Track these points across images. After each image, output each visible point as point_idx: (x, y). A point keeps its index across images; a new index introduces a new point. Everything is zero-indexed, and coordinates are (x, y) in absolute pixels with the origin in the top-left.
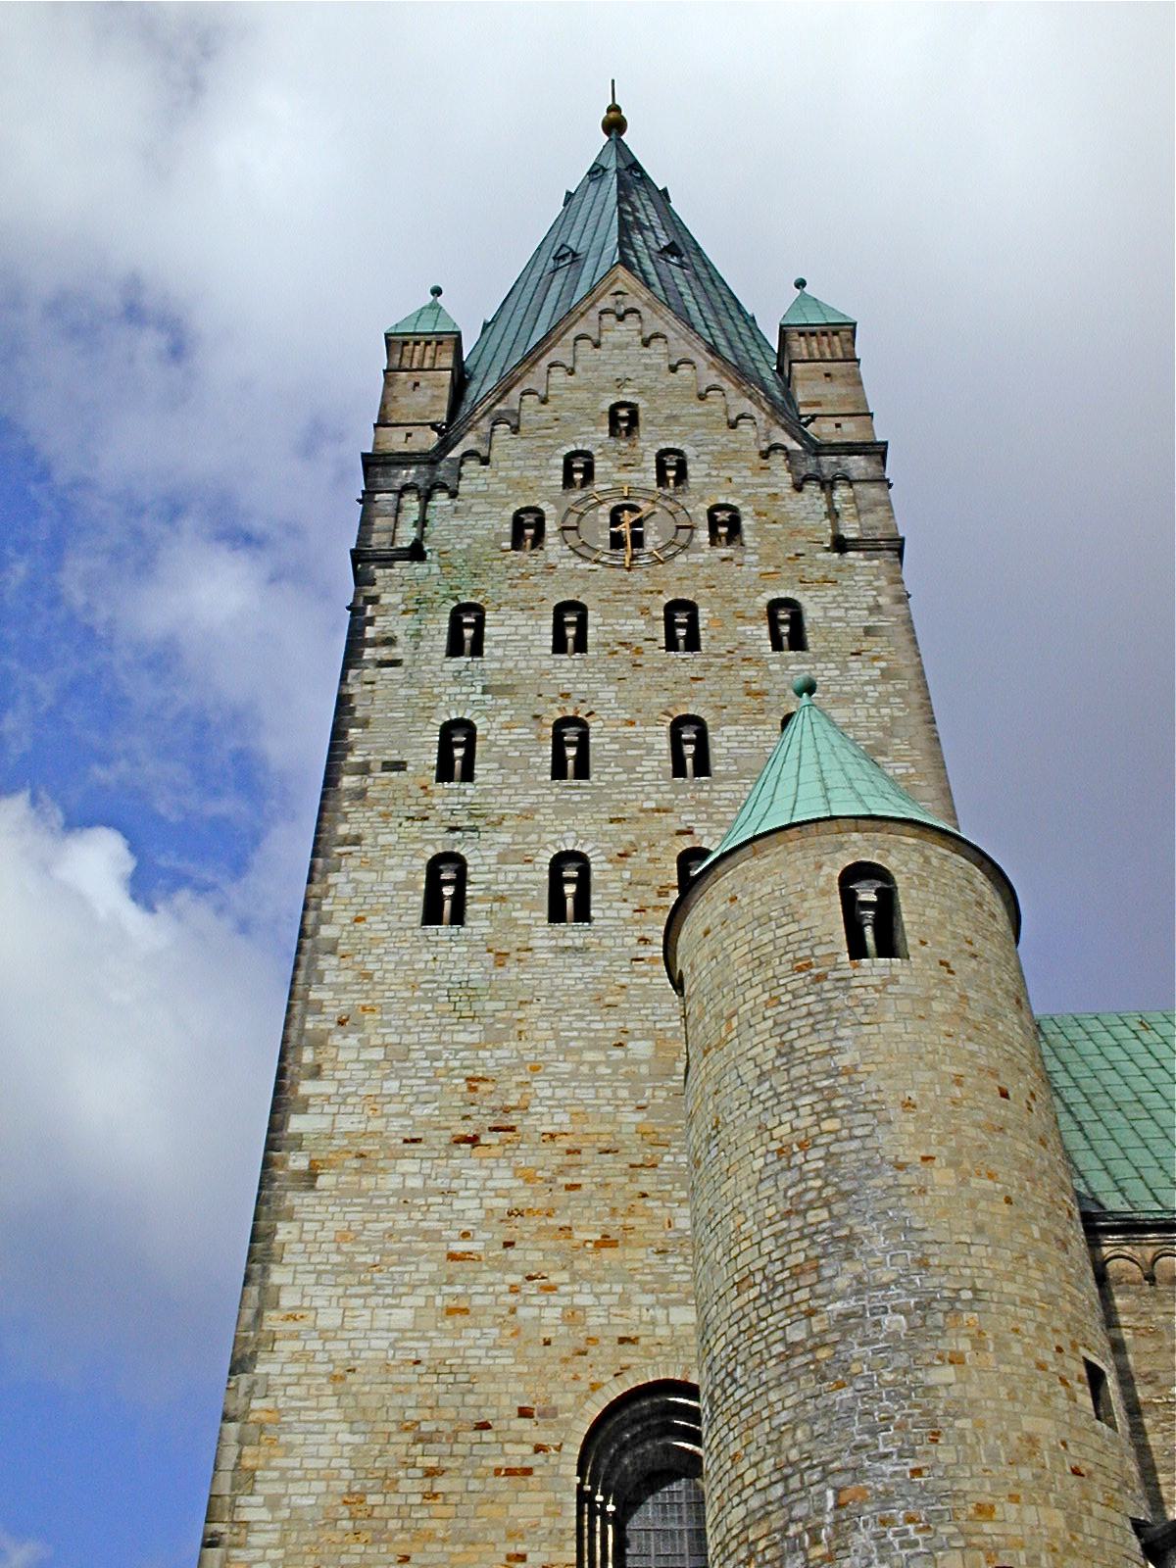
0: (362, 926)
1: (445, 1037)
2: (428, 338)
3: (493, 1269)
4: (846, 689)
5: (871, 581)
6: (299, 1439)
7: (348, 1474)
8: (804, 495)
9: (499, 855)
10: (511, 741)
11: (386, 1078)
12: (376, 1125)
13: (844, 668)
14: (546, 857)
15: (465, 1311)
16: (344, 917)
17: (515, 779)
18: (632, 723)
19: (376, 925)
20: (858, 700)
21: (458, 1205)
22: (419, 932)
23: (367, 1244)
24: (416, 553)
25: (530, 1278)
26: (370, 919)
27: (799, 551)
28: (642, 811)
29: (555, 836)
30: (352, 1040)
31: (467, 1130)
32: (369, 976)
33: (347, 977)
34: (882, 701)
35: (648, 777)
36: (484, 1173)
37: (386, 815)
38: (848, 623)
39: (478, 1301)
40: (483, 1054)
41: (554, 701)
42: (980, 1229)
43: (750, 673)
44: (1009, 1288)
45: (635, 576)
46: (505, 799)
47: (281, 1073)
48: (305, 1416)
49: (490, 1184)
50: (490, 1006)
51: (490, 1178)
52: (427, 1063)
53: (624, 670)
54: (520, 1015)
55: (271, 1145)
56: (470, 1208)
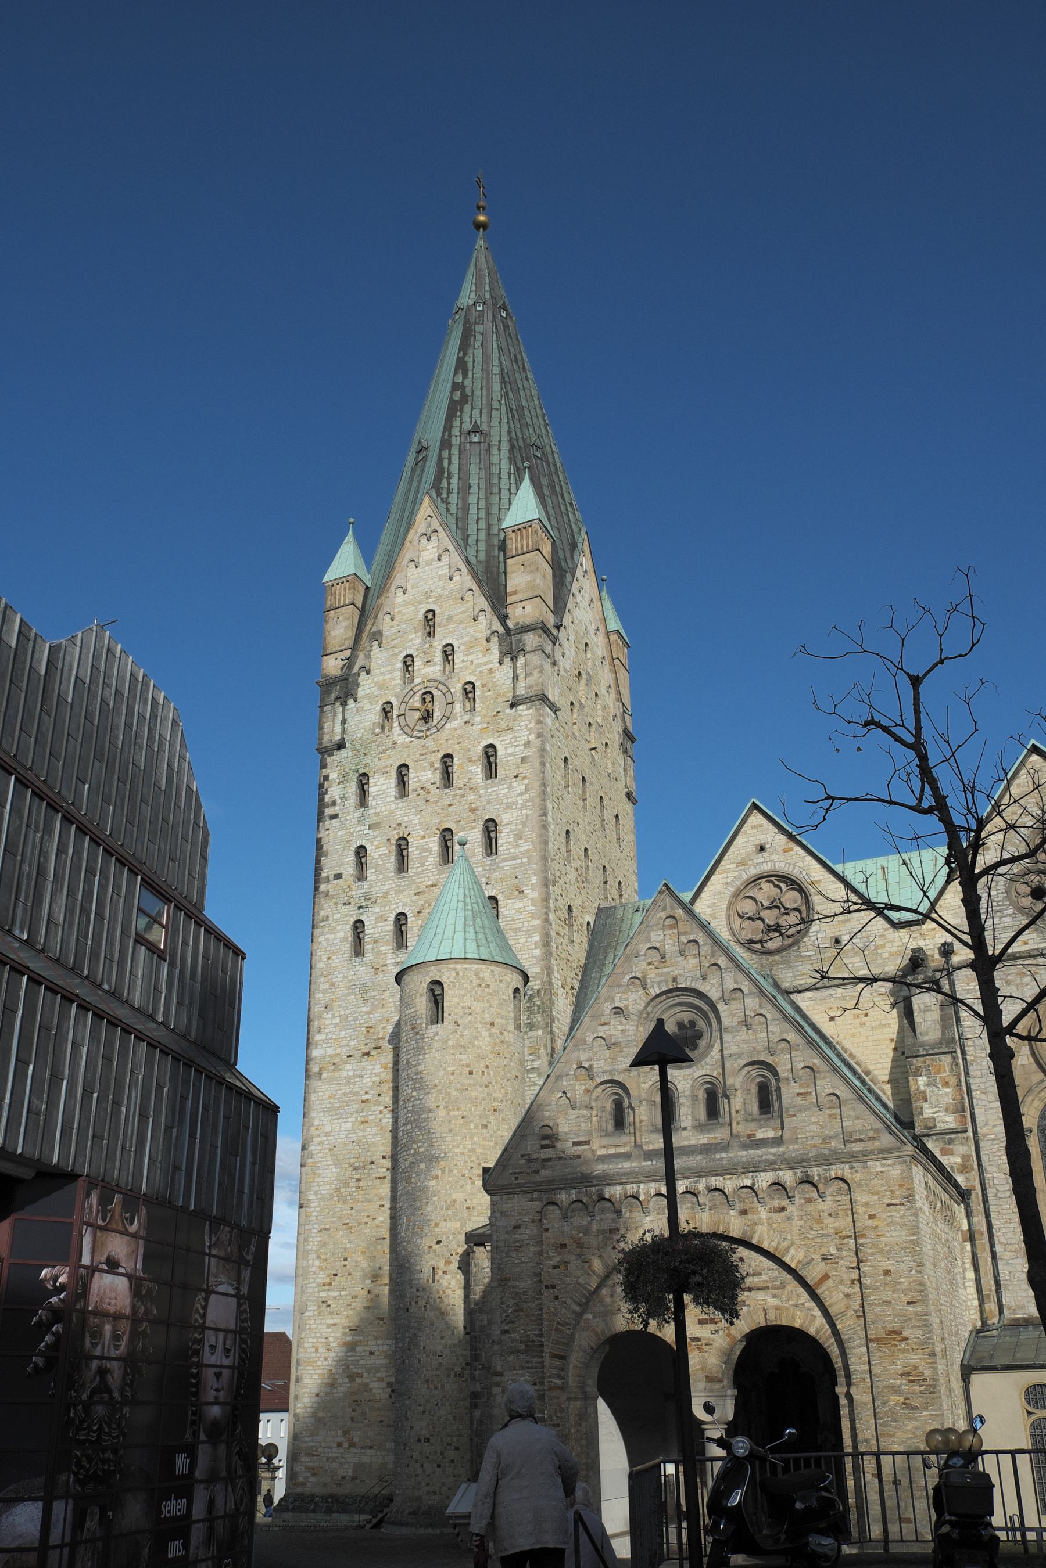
0: (331, 961)
1: (359, 1010)
2: (342, 580)
3: (375, 1105)
4: (510, 800)
5: (527, 725)
6: (321, 1172)
7: (335, 1182)
8: (503, 666)
9: (376, 919)
10: (380, 855)
11: (341, 1030)
12: (339, 1051)
13: (510, 787)
14: (392, 917)
15: (366, 1122)
16: (324, 958)
17: (381, 877)
18: (424, 837)
19: (335, 960)
20: (514, 807)
21: (364, 1081)
22: (349, 962)
23: (338, 1099)
24: (341, 746)
25: (386, 1107)
26: (333, 957)
27: (499, 709)
28: (427, 887)
29: (395, 906)
30: (330, 1015)
31: (366, 1050)
32: (333, 985)
33: (327, 986)
34: (524, 806)
35: (430, 867)
36: (372, 1067)
37: (336, 903)
38: (515, 756)
39: (370, 1117)
40: (371, 1016)
41: (395, 829)
42: (450, 1131)
43: (471, 797)
44: (457, 1150)
45: (429, 742)
46: (377, 888)
47: (308, 1033)
48: (323, 1163)
49: (374, 1071)
50: (373, 994)
51: (374, 1069)
52: (353, 1022)
53: (421, 803)
54: (383, 997)
55: (307, 1063)
56: (367, 1081)
